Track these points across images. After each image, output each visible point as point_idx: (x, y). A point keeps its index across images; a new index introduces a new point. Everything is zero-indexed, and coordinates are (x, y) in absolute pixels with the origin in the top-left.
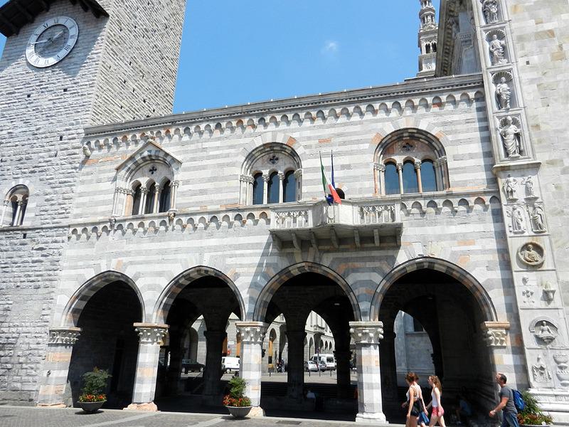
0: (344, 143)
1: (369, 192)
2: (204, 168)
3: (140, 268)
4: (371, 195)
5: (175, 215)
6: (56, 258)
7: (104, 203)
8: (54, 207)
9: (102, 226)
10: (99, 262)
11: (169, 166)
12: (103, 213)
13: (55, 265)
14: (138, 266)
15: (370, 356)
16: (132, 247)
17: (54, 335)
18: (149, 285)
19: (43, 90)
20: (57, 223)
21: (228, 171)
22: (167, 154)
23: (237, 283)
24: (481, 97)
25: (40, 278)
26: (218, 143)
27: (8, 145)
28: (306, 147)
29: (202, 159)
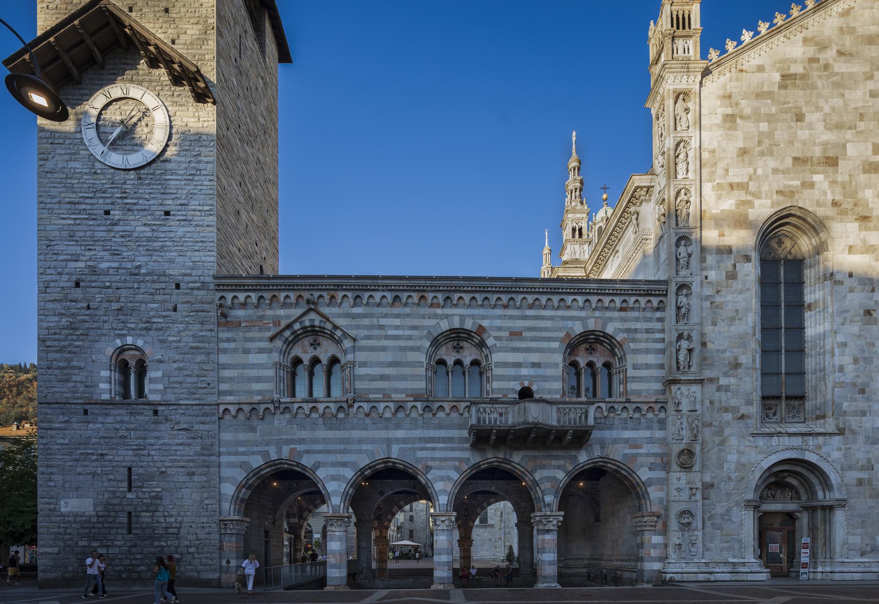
0: (535, 339)
1: (558, 393)
2: (384, 349)
3: (321, 458)
4: (558, 396)
6: (208, 441)
7: (259, 380)
8: (188, 379)
9: (262, 407)
10: (266, 448)
11: (338, 342)
12: (259, 392)
14: (317, 455)
16: (304, 434)
17: (226, 524)
18: (332, 476)
20: (199, 399)
21: (412, 356)
22: (336, 327)
23: (429, 476)
25: (192, 464)
26: (397, 322)
27: (93, 284)
28: (496, 338)
29: (379, 338)
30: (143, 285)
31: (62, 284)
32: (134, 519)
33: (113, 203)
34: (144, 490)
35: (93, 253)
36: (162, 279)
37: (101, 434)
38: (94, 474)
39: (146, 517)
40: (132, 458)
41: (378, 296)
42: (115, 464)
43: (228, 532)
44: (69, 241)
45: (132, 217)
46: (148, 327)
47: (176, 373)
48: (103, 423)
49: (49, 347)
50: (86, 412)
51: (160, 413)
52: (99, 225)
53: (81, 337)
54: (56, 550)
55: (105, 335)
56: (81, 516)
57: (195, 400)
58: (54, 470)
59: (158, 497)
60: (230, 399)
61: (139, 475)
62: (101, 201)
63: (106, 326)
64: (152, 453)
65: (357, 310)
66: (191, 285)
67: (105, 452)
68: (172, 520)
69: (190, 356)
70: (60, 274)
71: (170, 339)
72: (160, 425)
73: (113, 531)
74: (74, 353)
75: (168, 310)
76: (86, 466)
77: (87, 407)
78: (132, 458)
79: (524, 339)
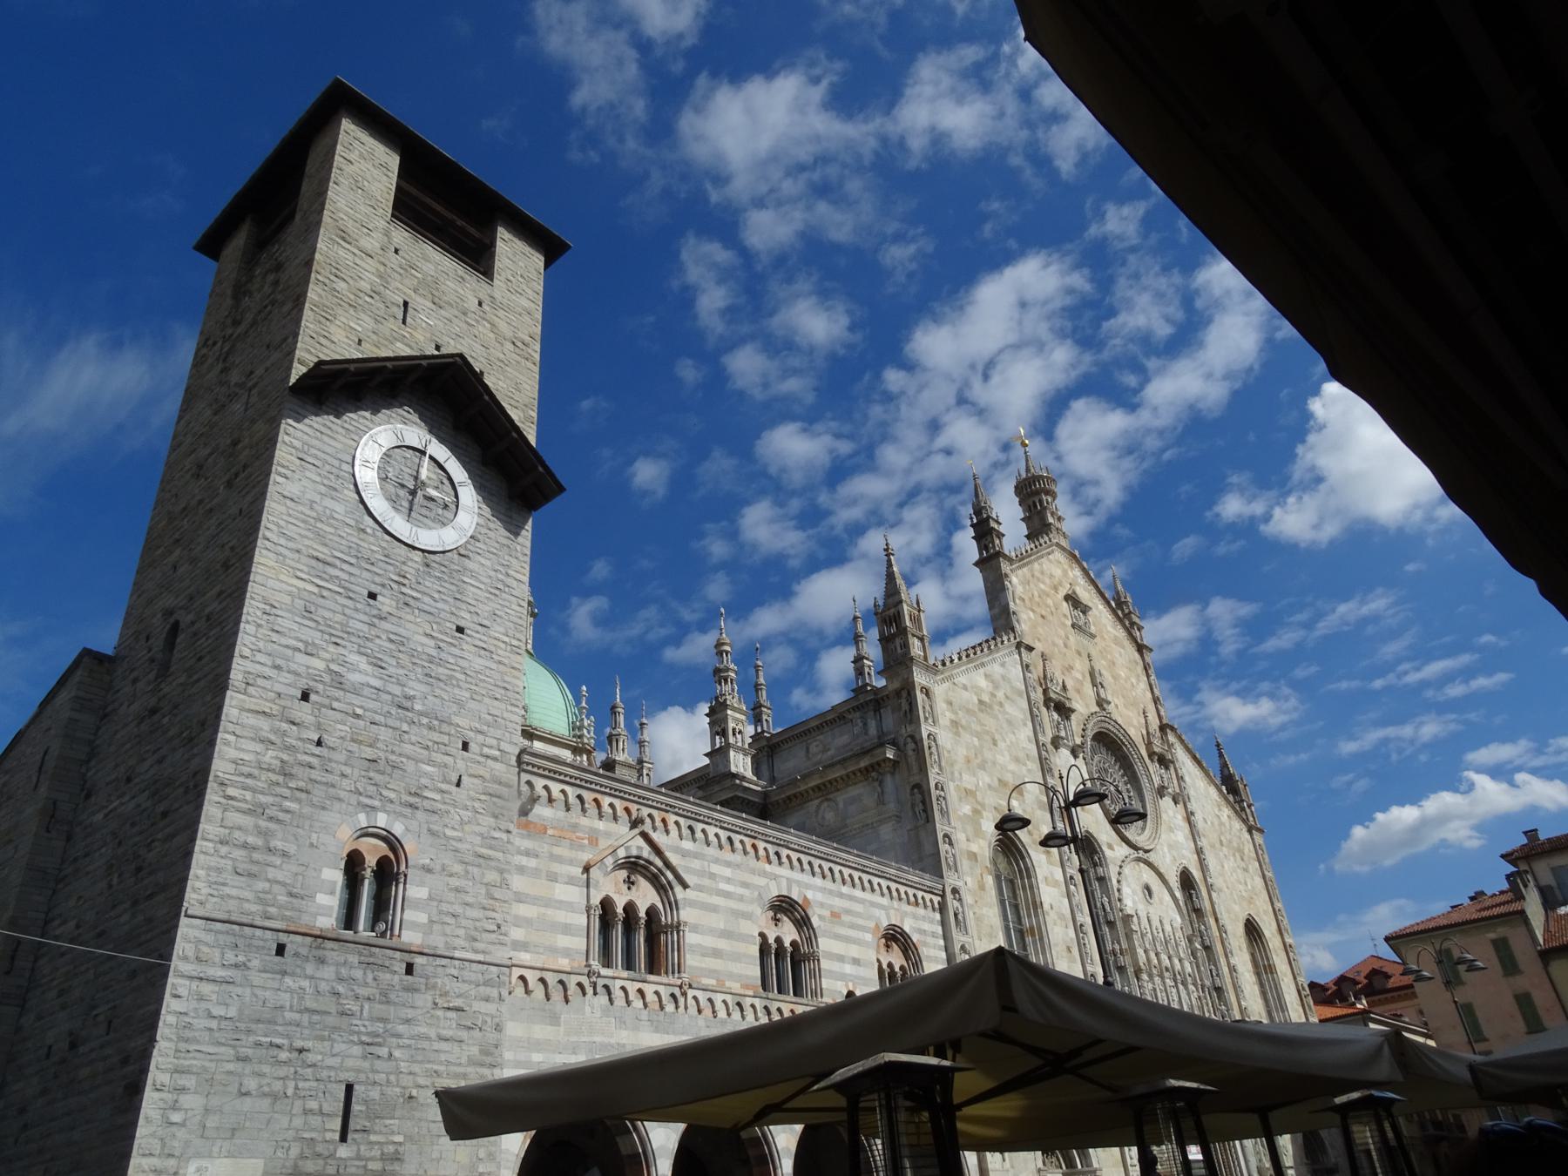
0: (852, 926)
2: (714, 909)
5: (690, 986)
6: (492, 1036)
7: (567, 929)
12: (567, 953)
13: (488, 1054)
19: (412, 602)
24: (942, 908)
26: (728, 872)
27: (336, 705)
30: (415, 729)
31: (278, 688)
33: (383, 586)
34: (373, 1138)
36: (445, 728)
37: (310, 1004)
38: (275, 1097)
41: (711, 830)
42: (325, 1074)
44: (304, 617)
45: (410, 617)
46: (414, 801)
47: (451, 896)
48: (312, 978)
49: (231, 798)
50: (281, 950)
52: (357, 610)
53: (298, 794)
55: (340, 800)
57: (476, 951)
58: (189, 1081)
60: (525, 957)
61: (366, 1102)
62: (366, 575)
63: (345, 782)
64: (397, 1053)
65: (687, 845)
66: (486, 750)
67: (308, 1044)
69: (476, 870)
70: (278, 667)
71: (449, 832)
72: (416, 996)
74: (279, 821)
75: (449, 783)
77: (283, 938)
79: (843, 924)
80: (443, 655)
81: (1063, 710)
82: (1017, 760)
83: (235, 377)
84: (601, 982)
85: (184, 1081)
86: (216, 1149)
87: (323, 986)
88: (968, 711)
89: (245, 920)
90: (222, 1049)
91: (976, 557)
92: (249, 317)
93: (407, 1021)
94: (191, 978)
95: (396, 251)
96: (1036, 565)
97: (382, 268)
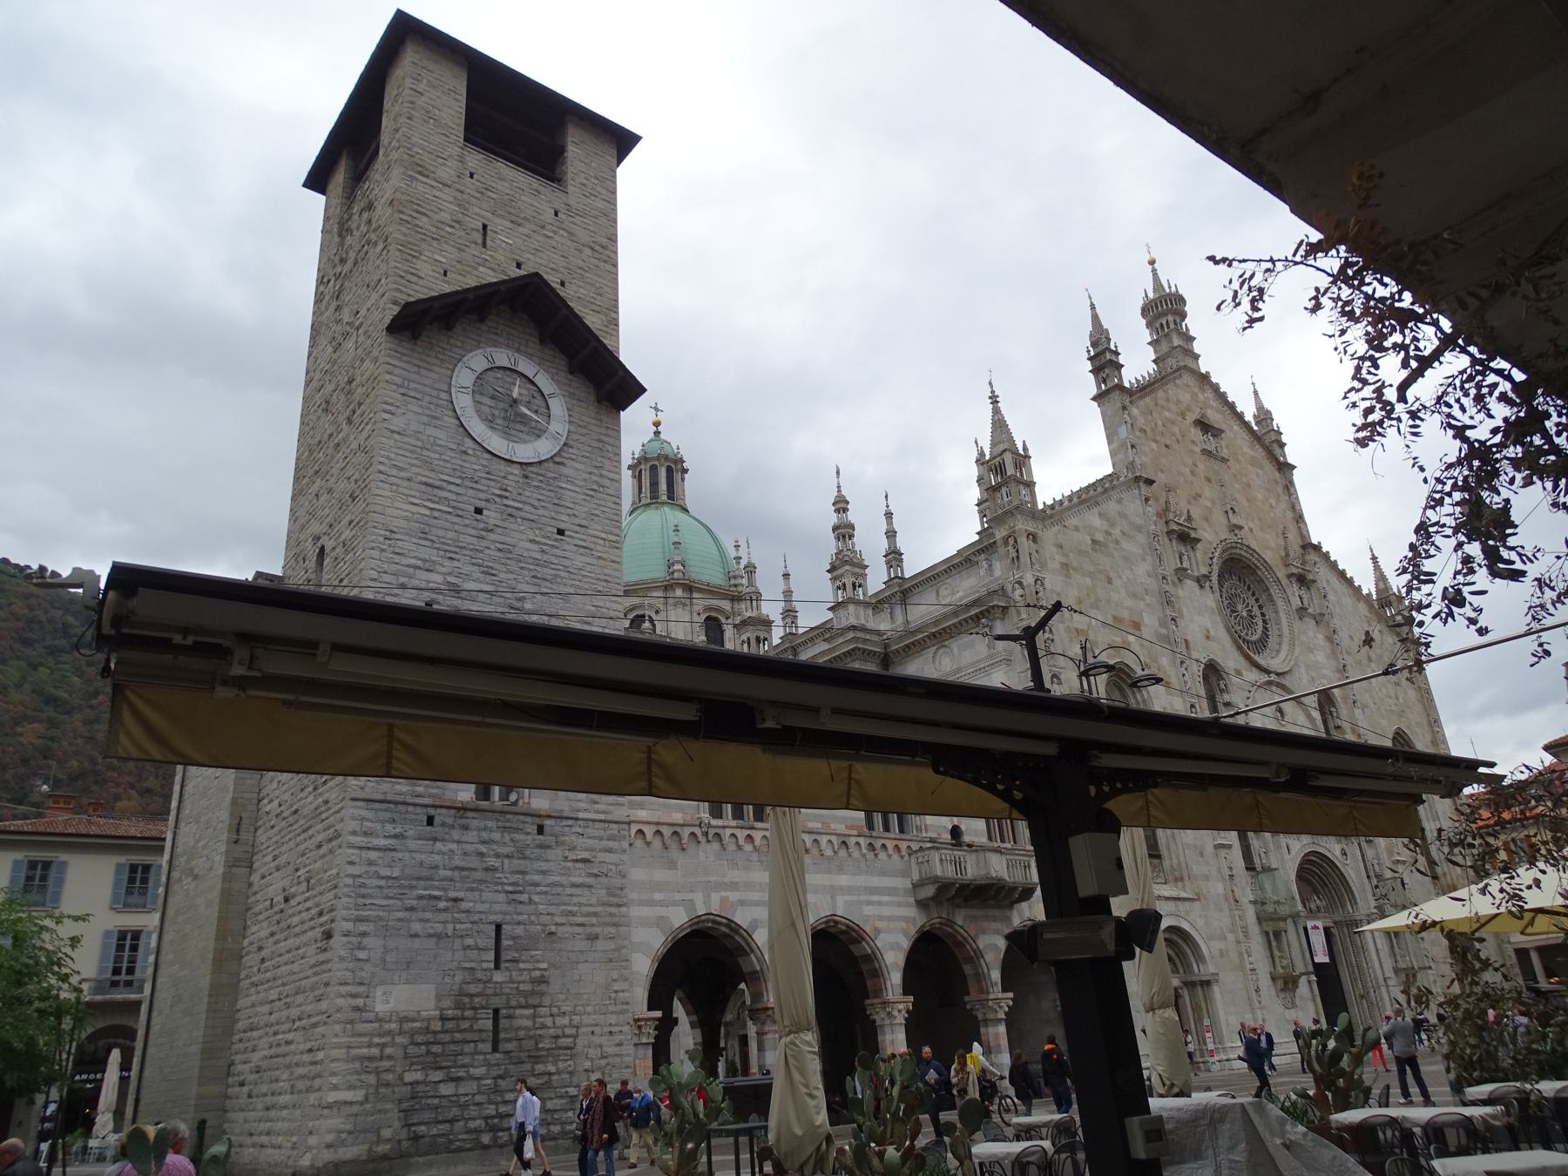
6: (617, 882)
10: (691, 896)
15: (997, 1035)
16: (735, 875)
19: (515, 513)
25: (594, 920)
32: (503, 1023)
33: (487, 501)
34: (522, 966)
35: (456, 564)
37: (458, 862)
38: (438, 936)
39: (523, 1018)
40: (505, 907)
42: (476, 917)
43: (644, 1040)
50: (430, 821)
51: (546, 829)
54: (358, 1095)
56: (413, 1020)
59: (543, 981)
61: (513, 938)
62: (471, 492)
64: (536, 898)
67: (461, 895)
68: (565, 1021)
73: (468, 1048)
76: (428, 921)
77: (431, 811)
78: (505, 907)
80: (546, 557)
81: (1185, 538)
82: (1134, 596)
83: (346, 316)
84: (712, 832)
85: (363, 927)
86: (396, 978)
87: (469, 847)
88: (1081, 552)
89: (398, 798)
90: (391, 902)
91: (1094, 391)
92: (352, 255)
93: (543, 873)
94: (361, 848)
95: (472, 176)
96: (1161, 393)
97: (458, 195)
